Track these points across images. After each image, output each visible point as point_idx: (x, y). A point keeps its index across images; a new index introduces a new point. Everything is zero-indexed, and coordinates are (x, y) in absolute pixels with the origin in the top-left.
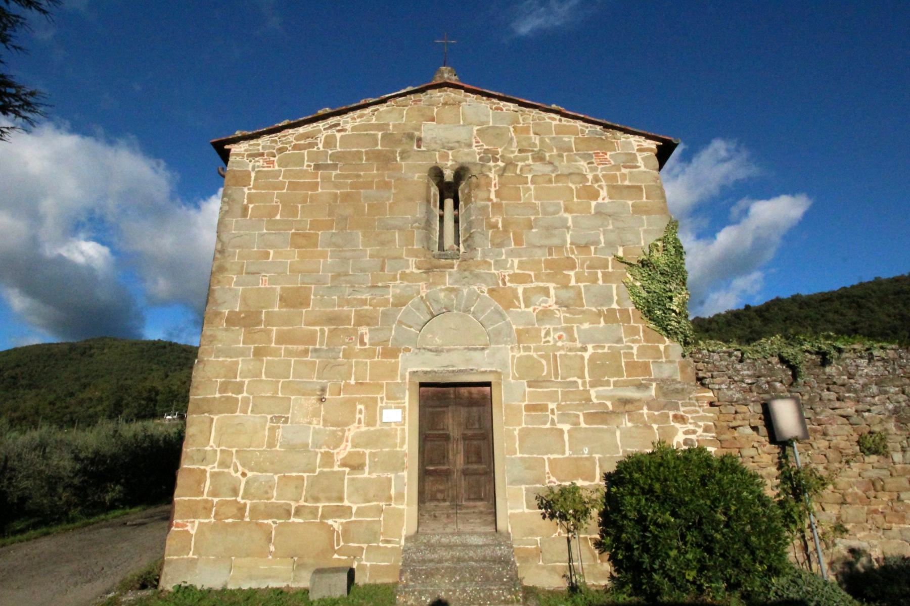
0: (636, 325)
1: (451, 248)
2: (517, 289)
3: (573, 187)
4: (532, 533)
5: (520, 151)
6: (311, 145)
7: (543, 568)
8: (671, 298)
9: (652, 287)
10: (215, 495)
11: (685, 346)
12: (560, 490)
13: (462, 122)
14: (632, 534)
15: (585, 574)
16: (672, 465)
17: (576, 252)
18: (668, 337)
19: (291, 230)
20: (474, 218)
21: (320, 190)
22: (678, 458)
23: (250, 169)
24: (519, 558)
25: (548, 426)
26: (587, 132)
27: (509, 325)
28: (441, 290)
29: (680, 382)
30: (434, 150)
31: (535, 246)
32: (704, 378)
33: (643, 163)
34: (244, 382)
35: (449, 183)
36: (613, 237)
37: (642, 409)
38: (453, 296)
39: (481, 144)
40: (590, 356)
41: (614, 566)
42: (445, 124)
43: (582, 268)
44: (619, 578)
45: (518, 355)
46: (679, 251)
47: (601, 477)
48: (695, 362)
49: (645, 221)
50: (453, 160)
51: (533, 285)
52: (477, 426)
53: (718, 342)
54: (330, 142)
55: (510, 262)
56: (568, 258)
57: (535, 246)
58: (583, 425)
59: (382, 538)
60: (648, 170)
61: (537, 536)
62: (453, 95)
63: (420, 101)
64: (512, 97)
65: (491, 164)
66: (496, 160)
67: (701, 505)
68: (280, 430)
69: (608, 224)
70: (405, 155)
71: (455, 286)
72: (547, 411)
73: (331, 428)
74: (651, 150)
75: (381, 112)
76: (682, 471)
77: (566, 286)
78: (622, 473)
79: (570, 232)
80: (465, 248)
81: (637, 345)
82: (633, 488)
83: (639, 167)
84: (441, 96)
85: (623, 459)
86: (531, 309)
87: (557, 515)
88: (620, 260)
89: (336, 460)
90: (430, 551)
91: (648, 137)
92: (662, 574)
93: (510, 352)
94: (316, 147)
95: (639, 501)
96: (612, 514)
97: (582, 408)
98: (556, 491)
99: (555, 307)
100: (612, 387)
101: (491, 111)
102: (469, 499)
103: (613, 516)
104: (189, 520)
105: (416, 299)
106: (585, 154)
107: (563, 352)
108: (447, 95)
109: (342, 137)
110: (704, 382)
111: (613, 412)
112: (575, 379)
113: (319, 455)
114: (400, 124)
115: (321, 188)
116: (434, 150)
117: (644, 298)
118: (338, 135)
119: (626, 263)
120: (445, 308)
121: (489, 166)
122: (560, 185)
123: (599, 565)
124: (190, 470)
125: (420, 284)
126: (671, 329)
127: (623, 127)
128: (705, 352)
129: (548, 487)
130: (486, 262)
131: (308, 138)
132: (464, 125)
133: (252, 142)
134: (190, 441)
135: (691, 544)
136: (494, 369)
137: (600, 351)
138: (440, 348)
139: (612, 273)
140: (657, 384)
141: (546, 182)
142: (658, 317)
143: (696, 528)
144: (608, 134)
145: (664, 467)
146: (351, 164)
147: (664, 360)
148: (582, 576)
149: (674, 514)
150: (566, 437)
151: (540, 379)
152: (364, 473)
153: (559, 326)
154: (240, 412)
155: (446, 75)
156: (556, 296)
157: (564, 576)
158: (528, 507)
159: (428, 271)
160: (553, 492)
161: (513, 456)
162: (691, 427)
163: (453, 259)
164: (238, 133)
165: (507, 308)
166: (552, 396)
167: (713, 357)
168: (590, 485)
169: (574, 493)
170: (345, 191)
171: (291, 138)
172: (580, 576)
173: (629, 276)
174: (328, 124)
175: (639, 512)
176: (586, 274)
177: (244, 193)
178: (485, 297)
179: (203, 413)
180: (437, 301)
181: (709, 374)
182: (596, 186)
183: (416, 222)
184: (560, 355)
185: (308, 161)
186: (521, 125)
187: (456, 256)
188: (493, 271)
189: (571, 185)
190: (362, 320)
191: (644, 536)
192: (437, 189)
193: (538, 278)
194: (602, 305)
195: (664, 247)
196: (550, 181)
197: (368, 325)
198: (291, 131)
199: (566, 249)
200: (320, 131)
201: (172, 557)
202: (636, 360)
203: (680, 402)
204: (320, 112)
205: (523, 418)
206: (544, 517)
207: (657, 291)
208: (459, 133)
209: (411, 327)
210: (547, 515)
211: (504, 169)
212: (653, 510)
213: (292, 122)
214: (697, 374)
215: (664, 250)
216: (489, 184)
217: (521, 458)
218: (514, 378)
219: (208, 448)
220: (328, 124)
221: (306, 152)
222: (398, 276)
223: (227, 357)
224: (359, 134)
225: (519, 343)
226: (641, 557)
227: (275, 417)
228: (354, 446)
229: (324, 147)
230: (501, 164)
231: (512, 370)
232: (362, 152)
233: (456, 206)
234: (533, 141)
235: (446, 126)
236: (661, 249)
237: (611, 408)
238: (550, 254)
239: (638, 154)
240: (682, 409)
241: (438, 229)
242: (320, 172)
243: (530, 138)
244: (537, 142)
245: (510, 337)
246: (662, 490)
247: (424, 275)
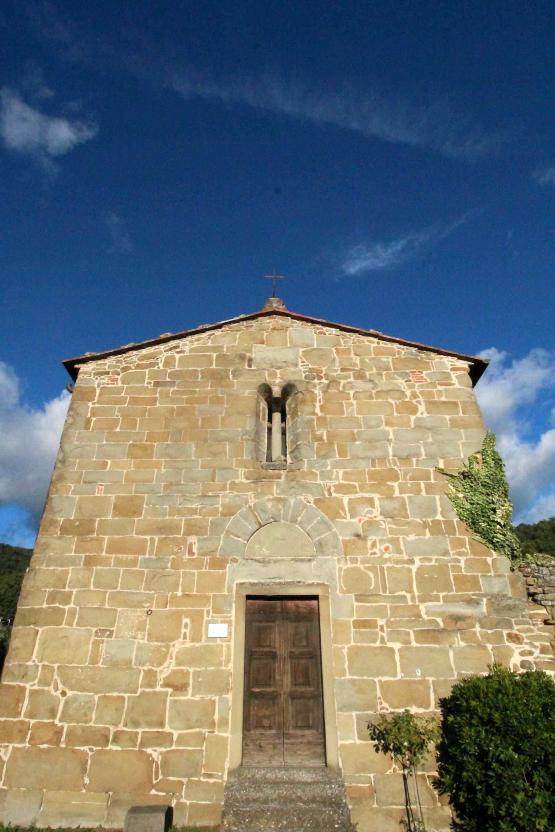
0: (462, 537)
1: (279, 459)
2: (342, 499)
3: (393, 402)
4: (364, 768)
5: (343, 370)
6: (153, 365)
7: (378, 811)
8: (494, 510)
9: (475, 499)
11: (513, 559)
12: (393, 719)
13: (289, 345)
14: (475, 775)
15: (425, 820)
16: (511, 692)
17: (398, 464)
18: (495, 550)
19: (129, 441)
20: (300, 430)
21: (158, 405)
22: (516, 683)
23: (96, 386)
24: (351, 798)
25: (378, 644)
26: (403, 353)
27: (335, 535)
28: (269, 500)
29: (511, 598)
30: (264, 369)
31: (359, 458)
32: (535, 594)
33: (457, 380)
34: (72, 592)
35: (277, 399)
36: (433, 449)
37: (474, 626)
38: (280, 506)
39: (307, 363)
40: (418, 569)
41: (456, 810)
42: (273, 346)
43: (405, 479)
44: (462, 825)
45: (345, 567)
46: (498, 463)
47: (436, 703)
48: (525, 576)
49: (463, 435)
50: (281, 378)
51: (358, 496)
52: (304, 643)
53: (546, 556)
54: (169, 362)
55: (335, 473)
56: (391, 469)
57: (359, 458)
58: (414, 644)
59: (203, 772)
60: (462, 387)
61: (370, 773)
62: (281, 321)
63: (252, 326)
64: (334, 323)
65: (316, 381)
66: (320, 378)
67: (546, 739)
68: (104, 645)
69: (428, 437)
70: (237, 373)
71: (282, 496)
72: (376, 628)
73: (156, 643)
74: (464, 369)
75: (216, 336)
76: (522, 699)
77: (390, 497)
78: (458, 700)
79: (392, 445)
80: (292, 459)
81: (465, 558)
82: (472, 718)
83: (454, 384)
84: (270, 323)
85: (457, 683)
86: (356, 520)
87: (391, 747)
88: (442, 472)
89: (159, 679)
91: (460, 358)
92: (510, 822)
93: (336, 563)
94: (157, 367)
95: (479, 732)
96: (450, 748)
97: (412, 624)
98: (389, 719)
99: (380, 518)
100: (441, 602)
101: (315, 335)
102: (296, 727)
103: (452, 750)
105: (244, 509)
106: (402, 373)
107: (390, 565)
108: (275, 321)
109: (180, 358)
110: (536, 598)
111: (444, 630)
112: (403, 593)
113: (142, 673)
114: (233, 346)
115: (160, 403)
116: (264, 369)
117: (468, 510)
118: (177, 356)
119: (447, 475)
120: (273, 518)
121: (314, 383)
122: (380, 400)
123: (439, 810)
124: (9, 687)
125: (249, 493)
126: (498, 542)
127: (436, 349)
128: (534, 566)
129: (381, 715)
130: (312, 473)
131: (150, 358)
132: (290, 348)
133: (99, 362)
135: (539, 786)
136: (321, 582)
137: (427, 564)
138: (267, 559)
139: (433, 484)
140: (488, 600)
141: (367, 398)
142: (483, 529)
143: (542, 766)
144: (423, 355)
145: (502, 694)
146: (188, 382)
147: (492, 574)
148: (421, 823)
149: (517, 750)
150: (397, 657)
151: (367, 593)
153: (385, 538)
154: (66, 625)
155: (275, 305)
156: (381, 506)
157: (401, 822)
158: (360, 738)
159: (257, 481)
160: (386, 721)
161: (343, 678)
162: (527, 648)
163: (280, 469)
164: (88, 355)
165: (332, 519)
166: (381, 612)
167: (542, 571)
168: (425, 713)
169: (409, 722)
170: (182, 405)
171: (135, 359)
172: (420, 822)
173: (452, 488)
174: (169, 346)
175: (479, 746)
176: (409, 485)
177: (88, 407)
178: (311, 507)
179: (29, 625)
180: (265, 511)
181: (540, 590)
182: (414, 401)
183: (246, 433)
184: (388, 567)
185: (148, 379)
186: (343, 347)
187: (283, 467)
188: (319, 481)
189: (390, 400)
191: (486, 775)
192: (266, 403)
193: (362, 488)
194: (426, 517)
195: (483, 459)
196: (371, 397)
197: (197, 534)
198: (135, 352)
199: (389, 460)
200: (161, 353)
202: (464, 574)
203: (513, 620)
204: (162, 336)
205: (352, 635)
206: (377, 750)
207: (480, 502)
208: (287, 354)
209: (239, 537)
210: (380, 748)
211: (328, 386)
212: (495, 744)
213: (137, 345)
214: (528, 589)
215: (483, 463)
216: (314, 400)
217: (352, 681)
218: (342, 591)
219: (30, 663)
220: (169, 346)
221: (147, 371)
222: (228, 486)
223: (57, 566)
224: (196, 355)
225: (346, 554)
226: (484, 800)
227: (100, 630)
228: (178, 664)
229: (164, 366)
230: (325, 381)
231: (339, 583)
232: (198, 371)
233: (283, 419)
234: (354, 361)
235: (274, 348)
236: (480, 461)
237: (442, 625)
238: (373, 466)
239: (452, 373)
240: (516, 627)
241: (266, 441)
242: (159, 389)
243: (352, 359)
244: (358, 362)
245: (336, 548)
246: (502, 720)
247: (253, 485)
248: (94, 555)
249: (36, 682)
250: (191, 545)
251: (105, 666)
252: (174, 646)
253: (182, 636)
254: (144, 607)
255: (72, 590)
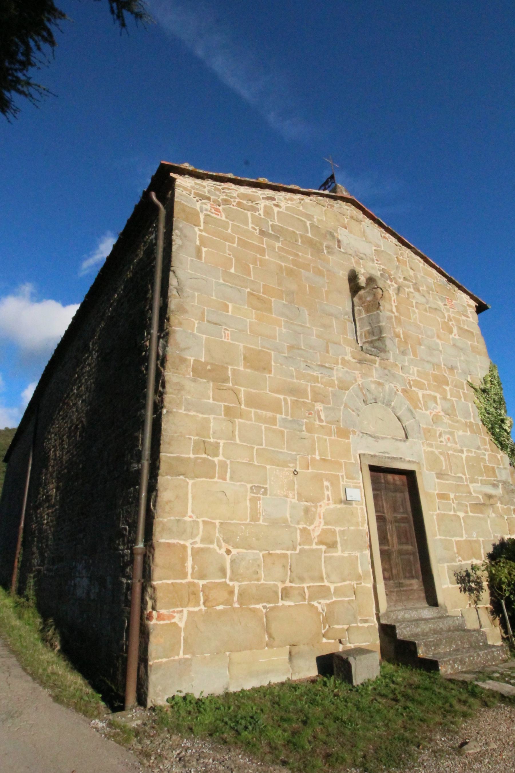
10: (202, 577)
29: (511, 485)
31: (424, 360)
34: (219, 443)
37: (497, 503)
59: (359, 618)
68: (261, 502)
73: (306, 503)
86: (428, 412)
89: (313, 537)
90: (415, 626)
93: (422, 446)
99: (442, 414)
102: (405, 577)
104: (177, 609)
113: (298, 531)
118: (276, 209)
124: (169, 545)
134: (167, 508)
137: (470, 454)
152: (337, 552)
154: (219, 478)
158: (451, 583)
179: (179, 475)
190: (318, 397)
197: (323, 402)
198: (233, 186)
201: (160, 660)
204: (261, 180)
206: (461, 591)
210: (462, 589)
219: (187, 519)
223: (197, 411)
227: (254, 486)
228: (326, 523)
247: (358, 365)
248: (233, 406)
249: (198, 539)
250: (318, 412)
251: (266, 524)
252: (321, 506)
253: (326, 498)
254: (290, 467)
255: (219, 441)
